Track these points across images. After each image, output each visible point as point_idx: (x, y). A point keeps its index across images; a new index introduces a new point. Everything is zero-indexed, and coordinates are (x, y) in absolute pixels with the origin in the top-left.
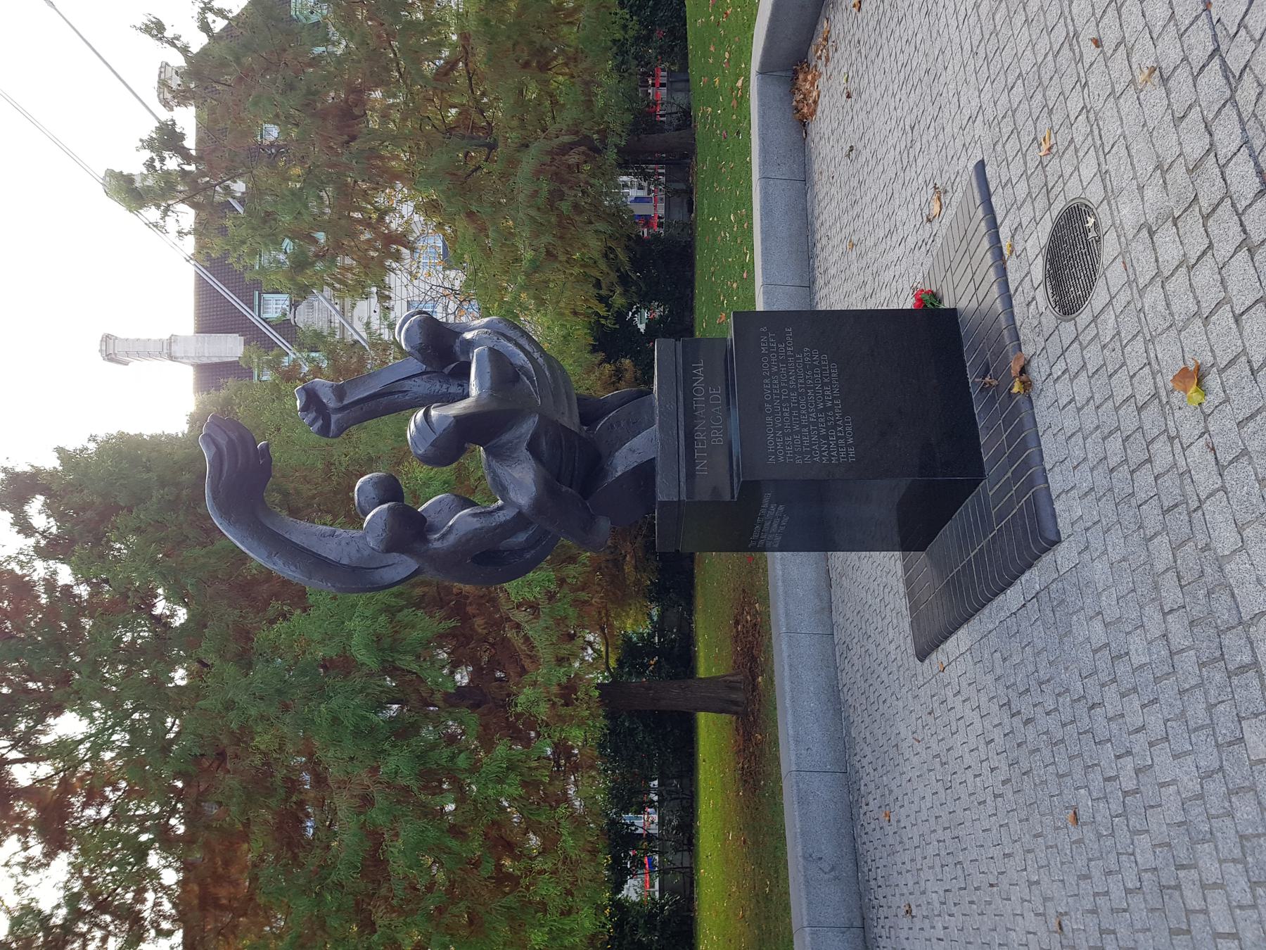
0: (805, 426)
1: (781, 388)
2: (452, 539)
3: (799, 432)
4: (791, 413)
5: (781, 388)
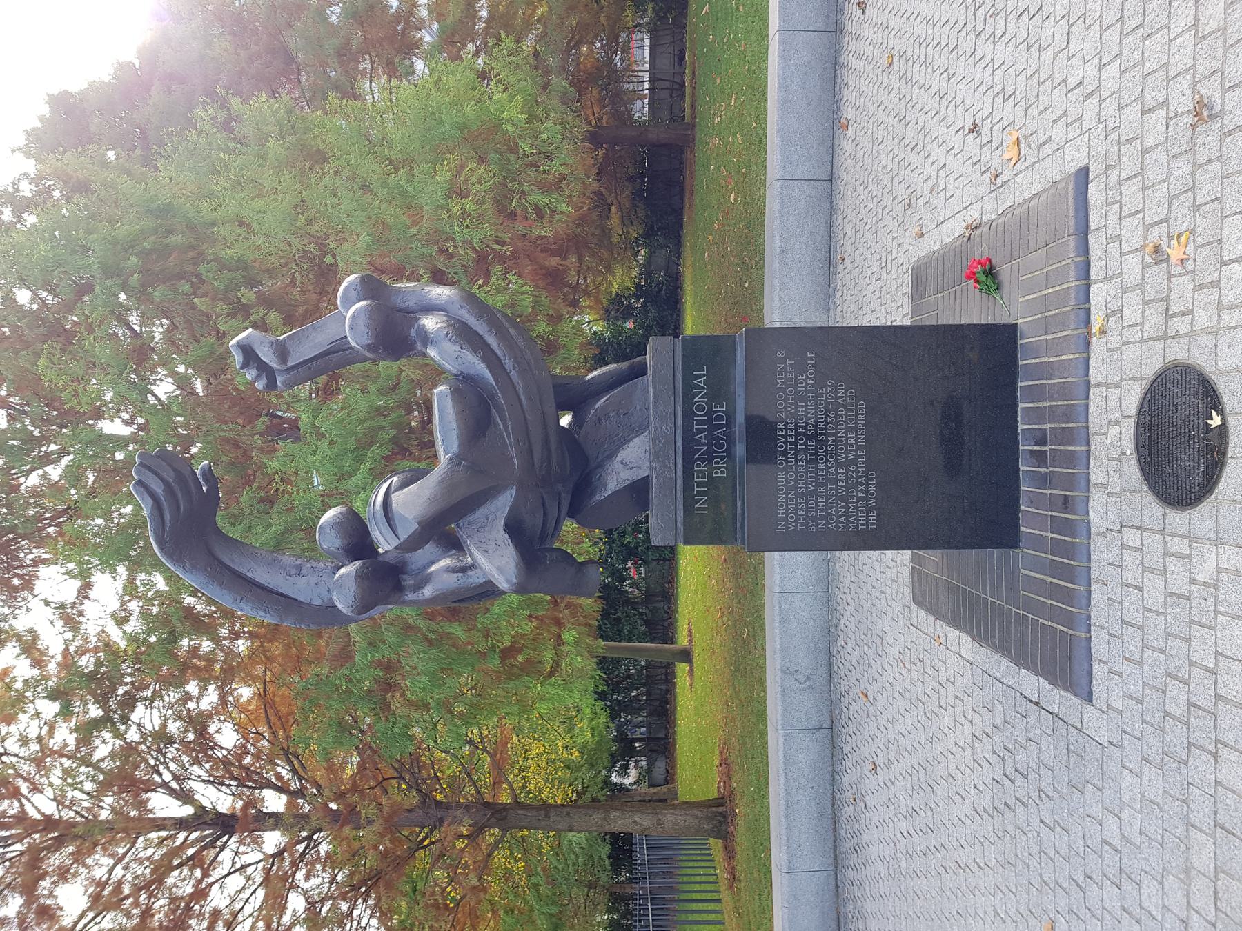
0: (822, 485)
1: (798, 434)
2: (427, 592)
3: (814, 493)
5: (798, 434)
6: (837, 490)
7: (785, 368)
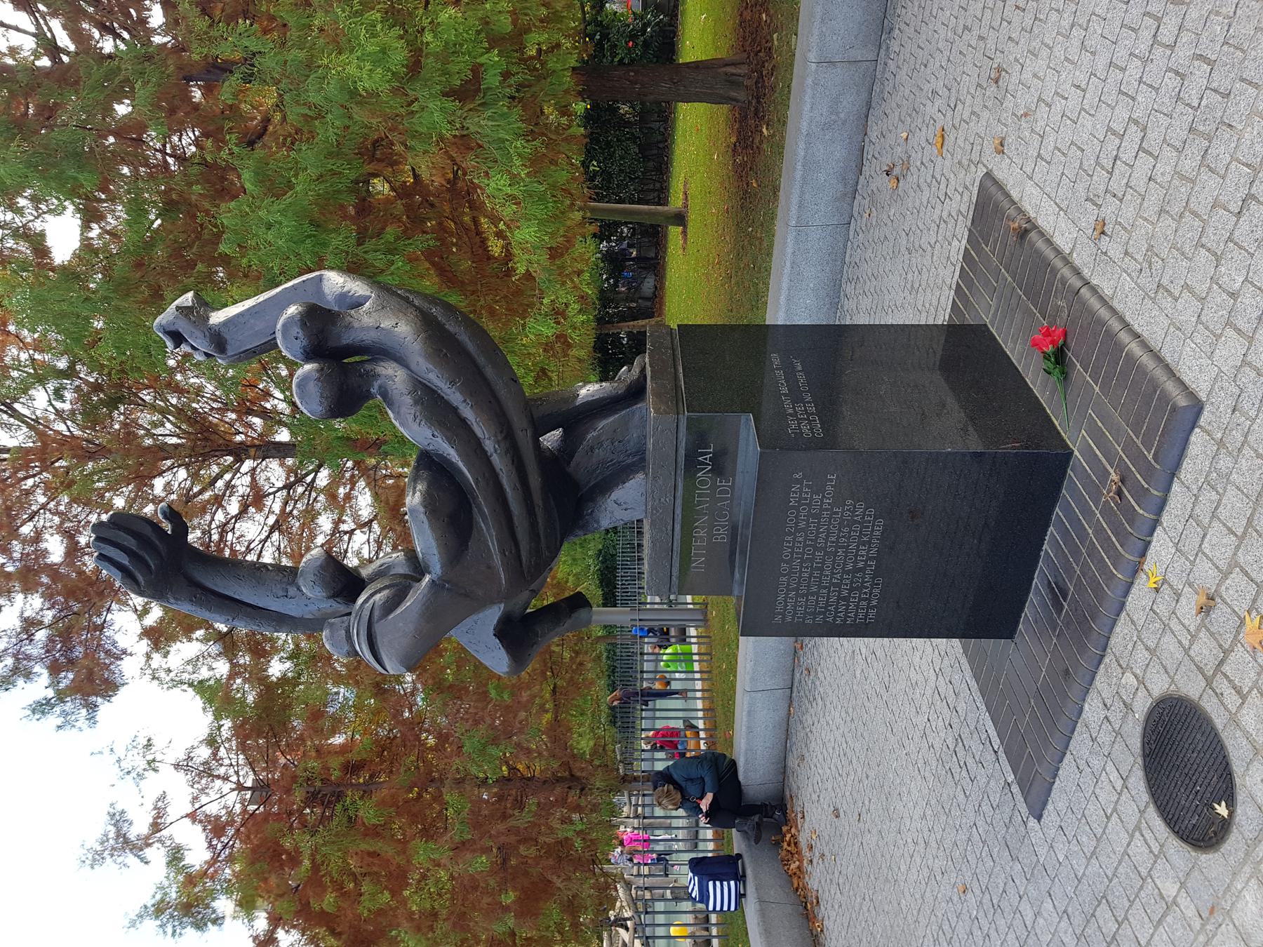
6: (839, 592)
7: (801, 489)
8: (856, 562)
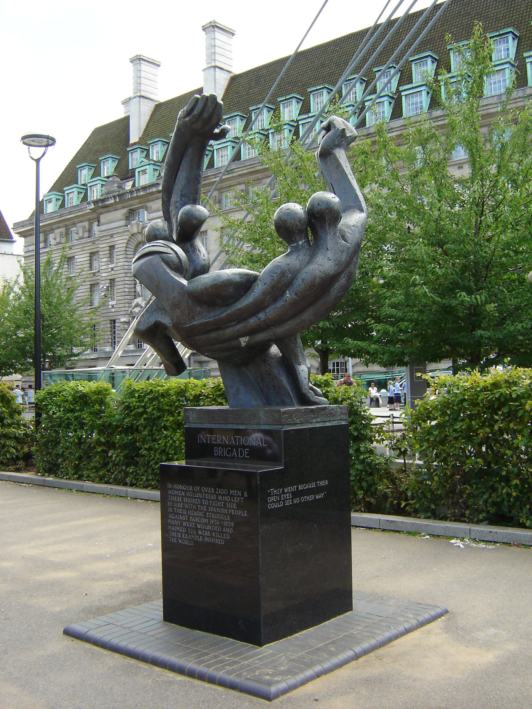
3: (184, 508)
4: (195, 504)
6: (185, 521)
7: (239, 496)
8: (201, 529)
